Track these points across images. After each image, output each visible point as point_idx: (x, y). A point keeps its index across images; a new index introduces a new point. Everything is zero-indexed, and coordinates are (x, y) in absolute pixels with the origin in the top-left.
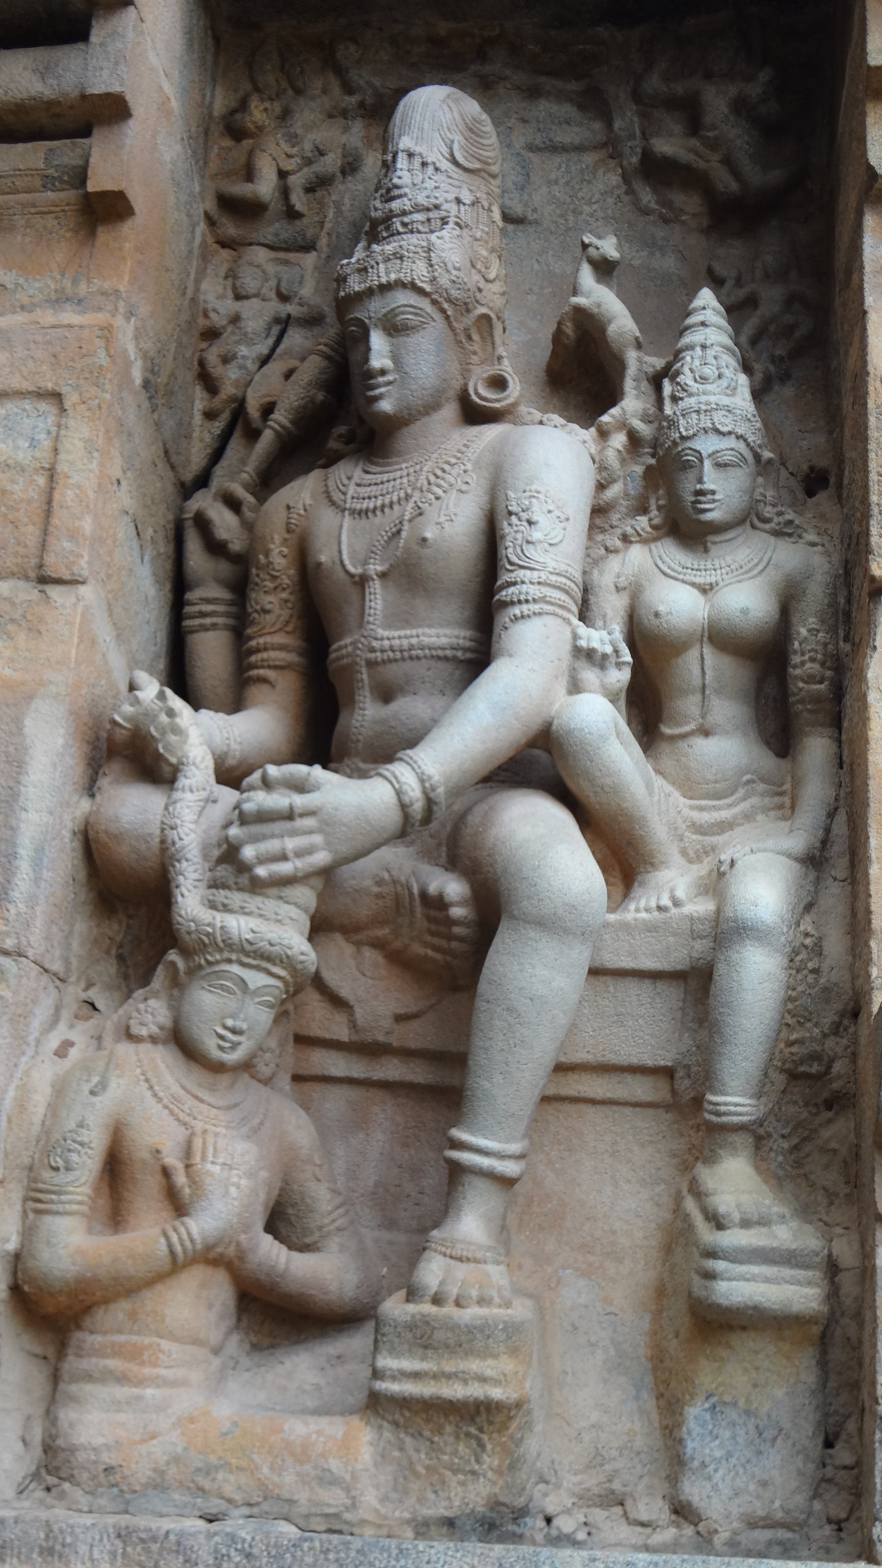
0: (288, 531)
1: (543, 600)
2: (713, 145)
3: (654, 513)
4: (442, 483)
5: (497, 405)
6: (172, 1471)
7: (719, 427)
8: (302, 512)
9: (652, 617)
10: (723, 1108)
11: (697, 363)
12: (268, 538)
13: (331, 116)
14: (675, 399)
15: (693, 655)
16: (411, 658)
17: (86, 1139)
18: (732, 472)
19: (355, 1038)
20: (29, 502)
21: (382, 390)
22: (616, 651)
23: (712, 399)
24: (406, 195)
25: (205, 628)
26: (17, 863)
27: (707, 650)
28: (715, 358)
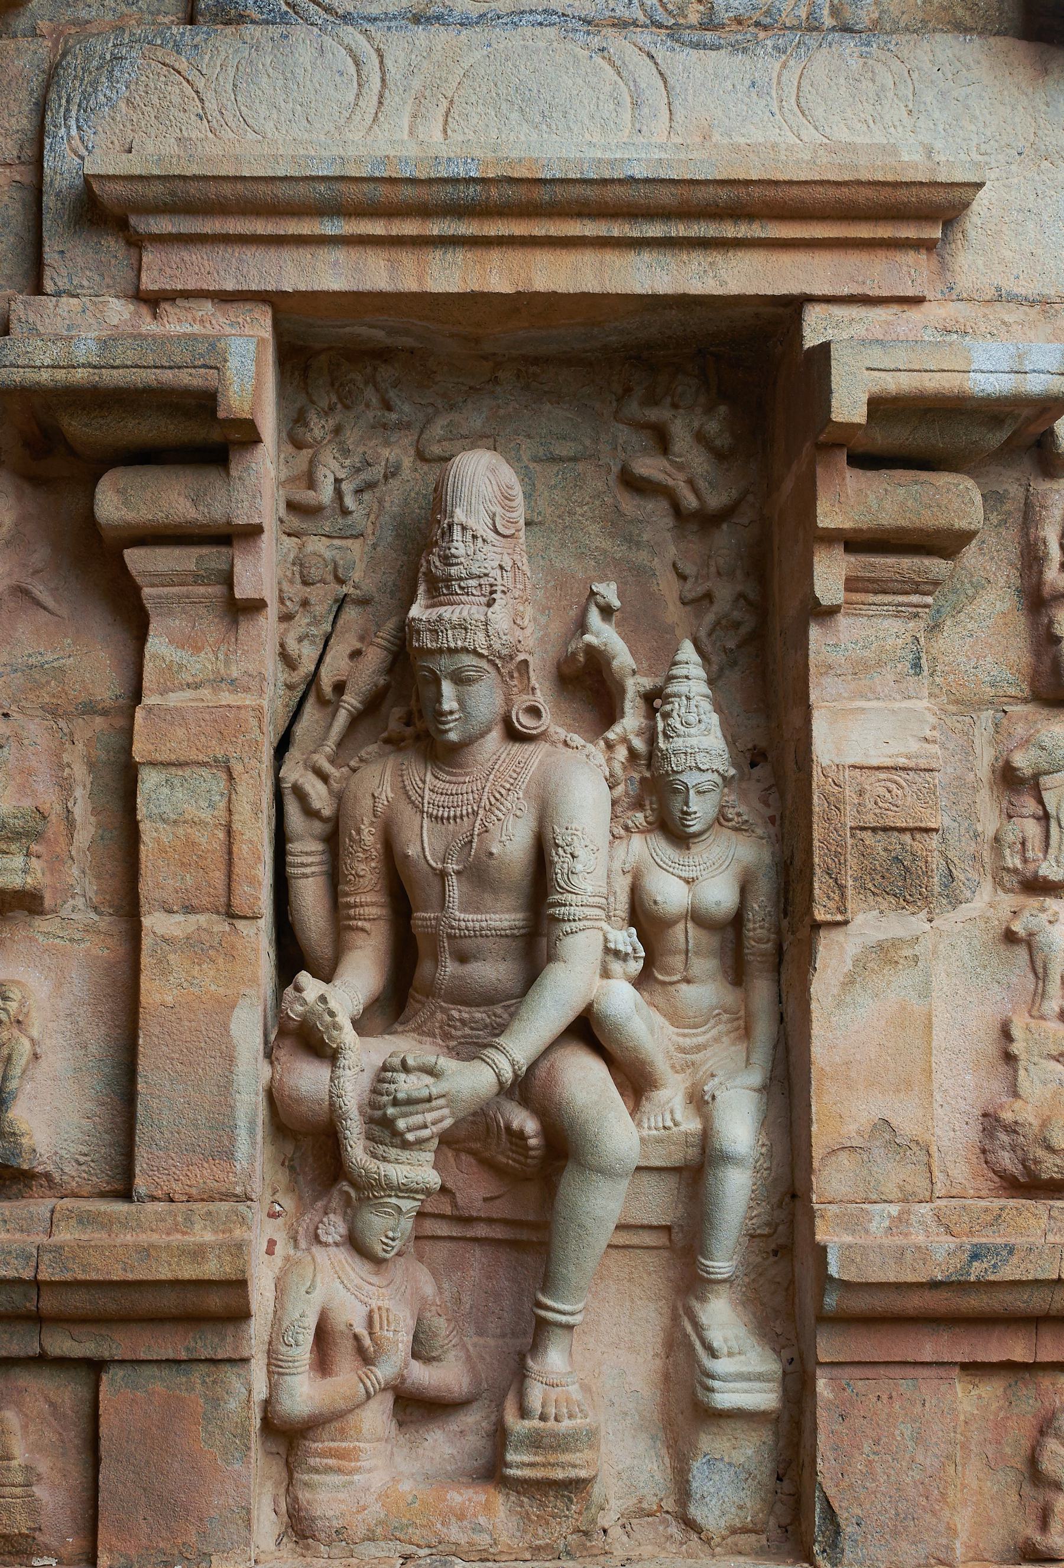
0: (375, 816)
1: (586, 918)
2: (680, 467)
3: (649, 812)
4: (501, 807)
5: (534, 732)
6: (379, 1530)
7: (700, 766)
8: (386, 803)
9: (651, 903)
10: (711, 1270)
11: (683, 710)
12: (359, 819)
13: (373, 427)
14: (667, 737)
15: (681, 926)
16: (481, 936)
17: (306, 1325)
18: (708, 795)
19: (456, 1213)
20: (213, 852)
21: (452, 725)
22: (634, 950)
23: (693, 741)
24: (462, 563)
25: (305, 876)
26: (237, 1131)
27: (690, 925)
28: (696, 706)
